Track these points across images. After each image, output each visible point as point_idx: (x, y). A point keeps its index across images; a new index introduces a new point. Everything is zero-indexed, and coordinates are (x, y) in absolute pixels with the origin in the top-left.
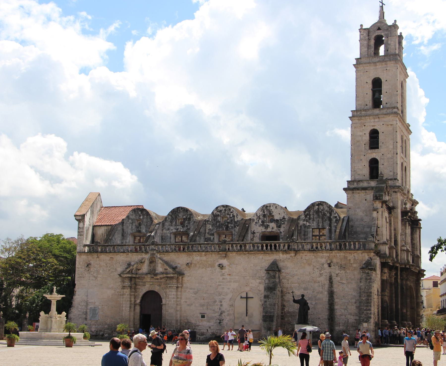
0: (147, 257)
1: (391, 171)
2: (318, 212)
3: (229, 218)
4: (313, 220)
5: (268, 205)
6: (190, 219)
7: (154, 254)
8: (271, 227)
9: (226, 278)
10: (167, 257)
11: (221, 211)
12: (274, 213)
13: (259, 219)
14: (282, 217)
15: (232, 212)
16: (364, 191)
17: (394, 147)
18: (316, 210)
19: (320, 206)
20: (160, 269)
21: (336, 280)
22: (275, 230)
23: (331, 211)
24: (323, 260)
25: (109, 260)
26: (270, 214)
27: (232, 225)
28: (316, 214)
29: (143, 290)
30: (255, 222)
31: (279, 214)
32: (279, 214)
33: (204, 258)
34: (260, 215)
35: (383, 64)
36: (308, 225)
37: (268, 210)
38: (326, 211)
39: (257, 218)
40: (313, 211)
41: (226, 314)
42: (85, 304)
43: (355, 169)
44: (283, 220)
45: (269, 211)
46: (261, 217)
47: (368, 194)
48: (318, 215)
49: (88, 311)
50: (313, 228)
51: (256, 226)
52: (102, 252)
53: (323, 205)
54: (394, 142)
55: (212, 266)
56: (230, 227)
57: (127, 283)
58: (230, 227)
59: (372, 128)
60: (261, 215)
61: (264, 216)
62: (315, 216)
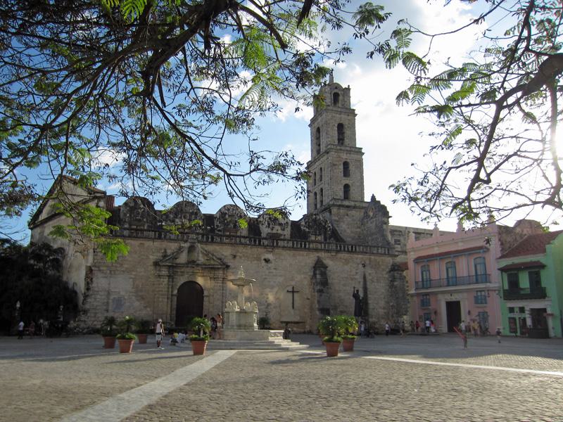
0: (187, 245)
6: (196, 214)
7: (195, 243)
9: (272, 272)
10: (210, 248)
11: (229, 210)
20: (202, 259)
21: (369, 278)
22: (280, 232)
24: (358, 261)
25: (138, 246)
29: (181, 280)
33: (250, 251)
41: (272, 307)
42: (106, 293)
49: (110, 301)
52: (130, 237)
55: (258, 259)
57: (164, 272)
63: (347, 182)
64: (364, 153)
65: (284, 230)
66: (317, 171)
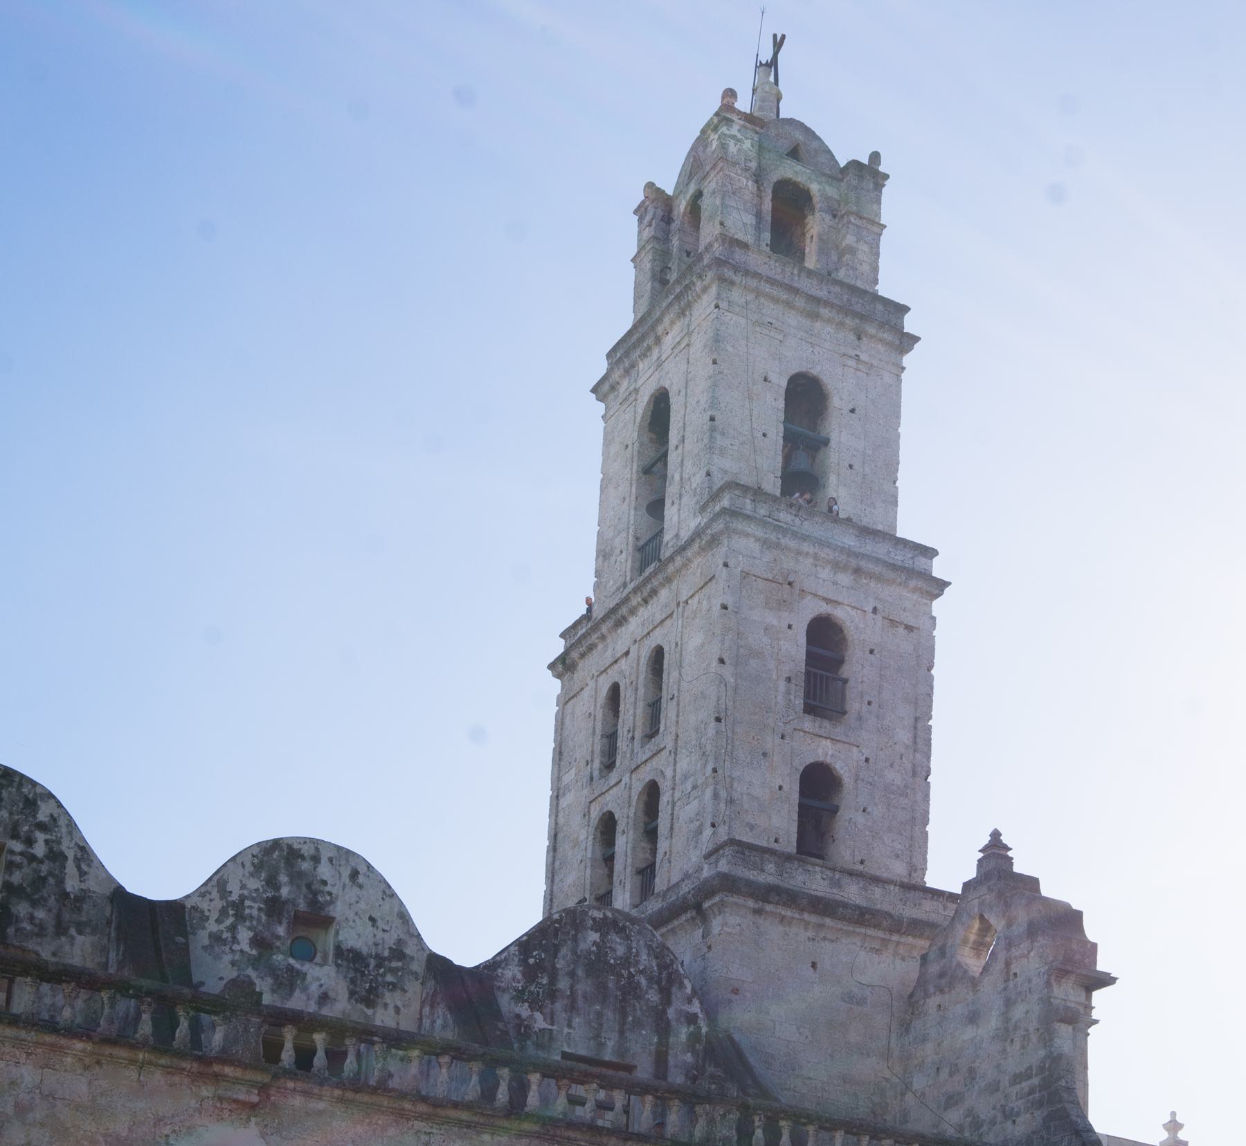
1: (897, 856)
2: (597, 964)
3: (18, 859)
4: (572, 1007)
5: (306, 850)
8: (314, 988)
12: (339, 904)
13: (240, 917)
14: (390, 940)
15: (42, 827)
16: (813, 919)
17: (915, 743)
18: (590, 952)
19: (614, 938)
23: (670, 980)
26: (313, 903)
27: (40, 914)
28: (588, 973)
30: (211, 935)
31: (372, 919)
32: (372, 919)
34: (242, 899)
35: (849, 321)
36: (542, 1030)
37: (301, 874)
38: (641, 972)
39: (223, 912)
40: (574, 952)
43: (735, 795)
44: (394, 964)
45: (309, 886)
46: (253, 909)
47: (824, 939)
48: (602, 989)
50: (567, 1049)
51: (217, 958)
53: (628, 938)
54: (916, 719)
56: (27, 926)
58: (27, 926)
59: (824, 608)
60: (254, 900)
61: (274, 907)
62: (585, 986)
63: (823, 751)
64: (942, 585)
65: (370, 999)
66: (633, 672)
